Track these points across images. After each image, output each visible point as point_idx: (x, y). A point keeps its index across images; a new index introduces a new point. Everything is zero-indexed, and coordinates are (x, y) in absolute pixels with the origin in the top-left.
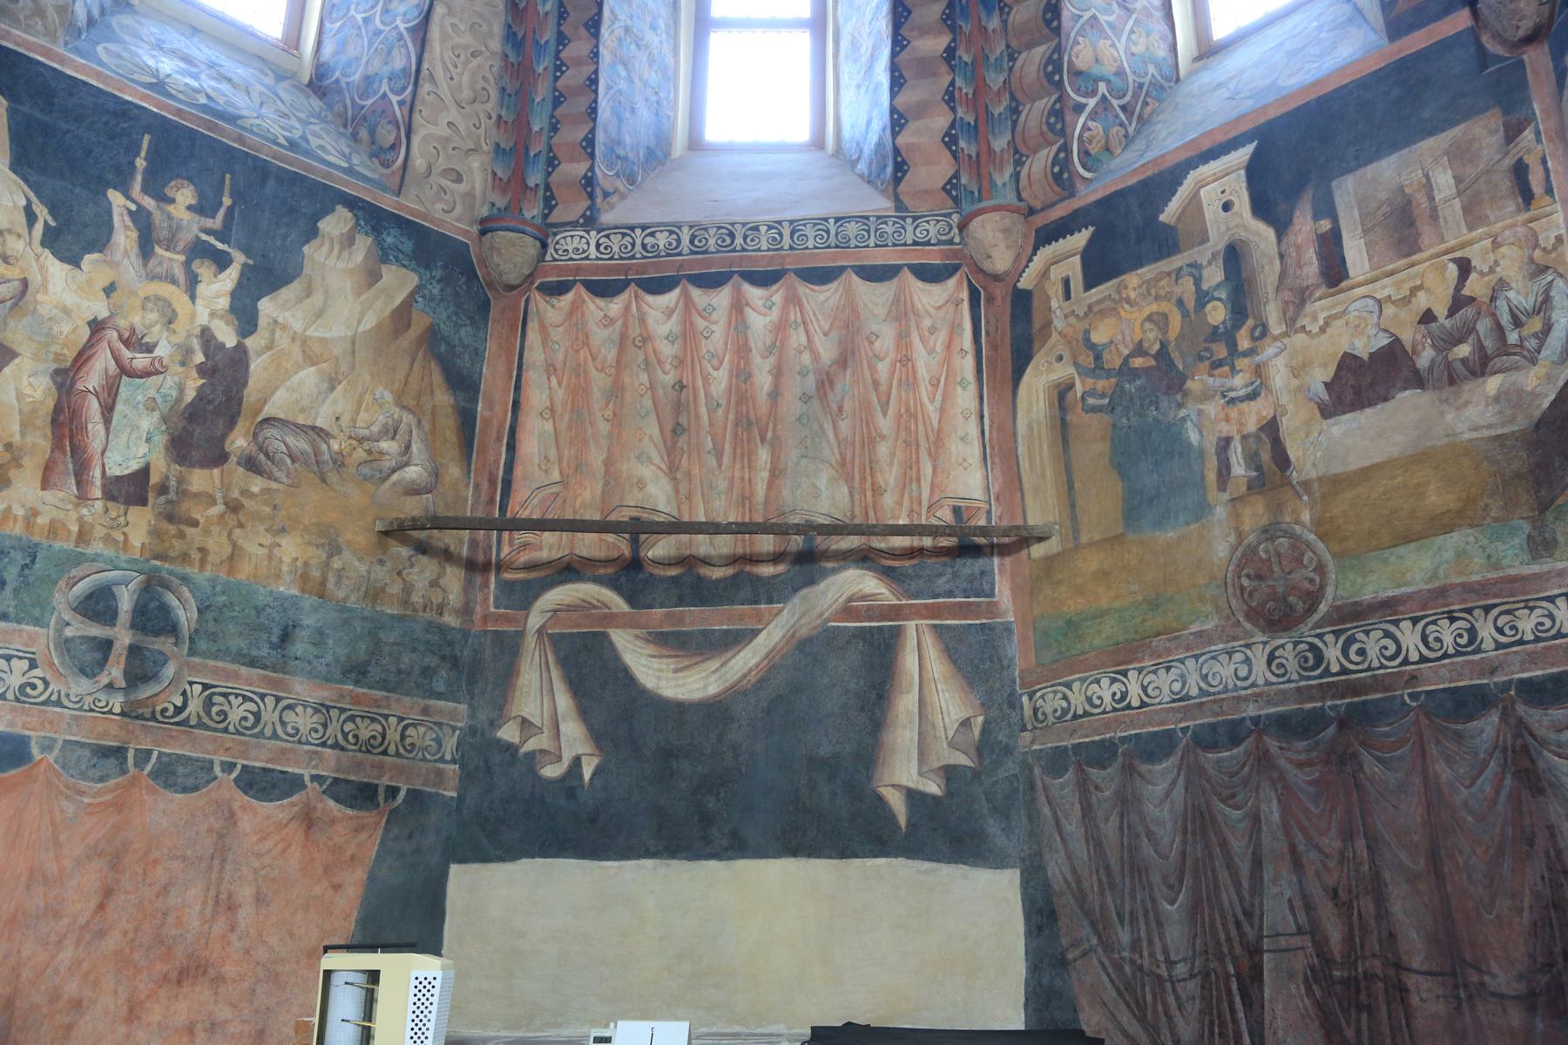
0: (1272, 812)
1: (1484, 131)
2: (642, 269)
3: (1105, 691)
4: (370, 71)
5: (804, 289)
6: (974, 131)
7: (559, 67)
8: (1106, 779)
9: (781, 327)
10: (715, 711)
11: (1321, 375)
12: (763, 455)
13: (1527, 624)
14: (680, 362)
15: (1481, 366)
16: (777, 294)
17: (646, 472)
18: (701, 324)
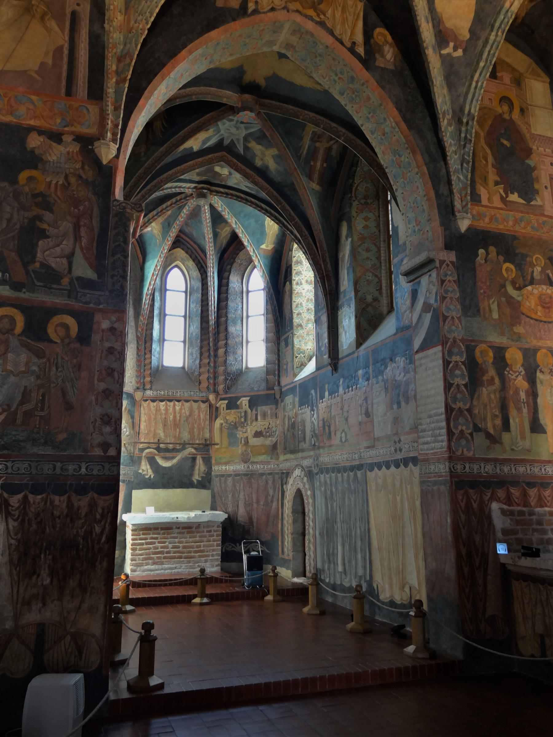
0: (242, 485)
1: (274, 407)
2: (159, 397)
3: (224, 468)
5: (185, 403)
8: (223, 479)
9: (181, 409)
10: (170, 468)
11: (253, 432)
12: (178, 430)
13: (269, 466)
14: (165, 414)
15: (269, 436)
16: (180, 403)
17: (160, 432)
18: (169, 408)
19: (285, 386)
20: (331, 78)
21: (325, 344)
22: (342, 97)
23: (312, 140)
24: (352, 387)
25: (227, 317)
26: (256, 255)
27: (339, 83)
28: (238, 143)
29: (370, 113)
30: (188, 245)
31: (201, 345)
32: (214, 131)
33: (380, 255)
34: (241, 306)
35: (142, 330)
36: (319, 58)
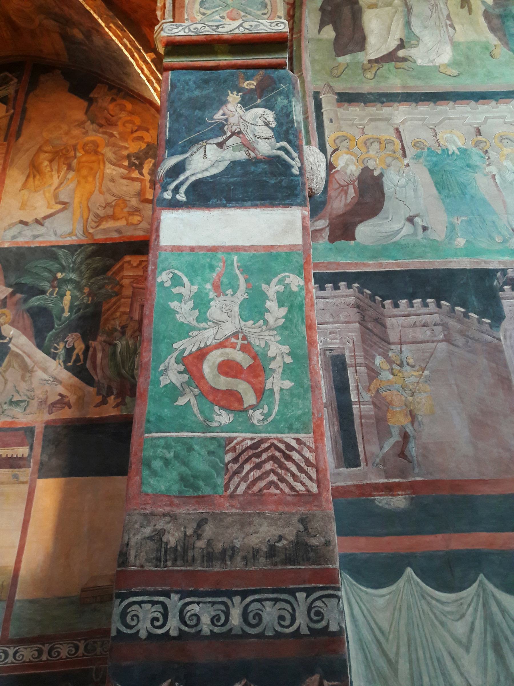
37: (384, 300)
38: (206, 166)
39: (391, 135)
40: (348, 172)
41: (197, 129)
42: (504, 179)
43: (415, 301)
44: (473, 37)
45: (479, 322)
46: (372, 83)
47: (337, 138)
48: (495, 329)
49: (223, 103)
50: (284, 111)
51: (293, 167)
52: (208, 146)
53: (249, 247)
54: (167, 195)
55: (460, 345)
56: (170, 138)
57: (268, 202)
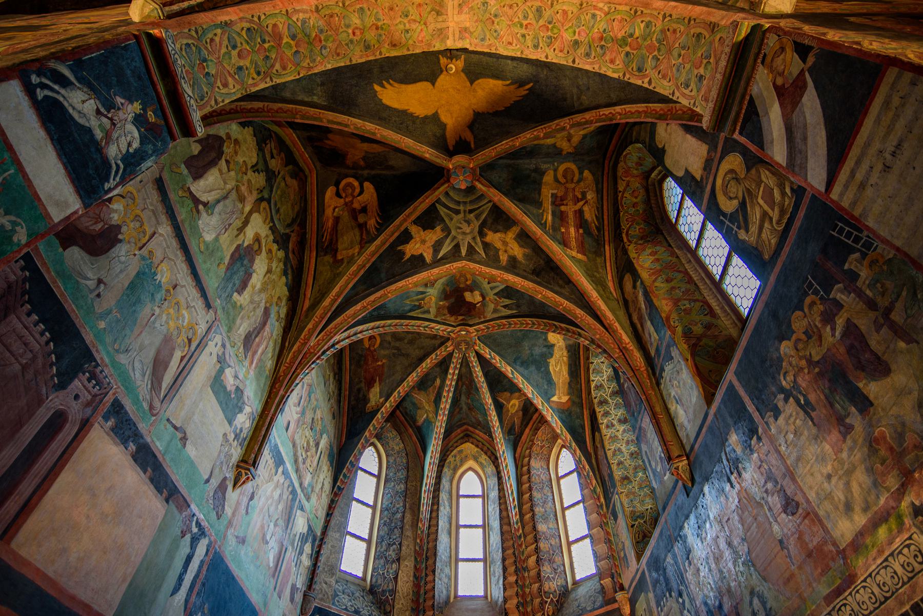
4: (385, 587)
6: (523, 605)
7: (426, 583)
19: (630, 587)
20: (518, 35)
21: (660, 458)
22: (539, 50)
23: (553, 203)
24: (729, 480)
25: (532, 510)
26: (547, 409)
27: (529, 35)
28: (476, 243)
29: (575, 32)
30: (477, 437)
31: (503, 556)
32: (442, 230)
33: (691, 278)
34: (551, 497)
35: (421, 540)
36: (496, 21)
37: (27, 302)
38: (76, 106)
39: (149, 232)
40: (111, 216)
41: (102, 85)
42: (154, 323)
43: (41, 325)
44: (224, 247)
45: (52, 377)
46: (177, 198)
47: (131, 193)
48: (53, 390)
49: (131, 101)
50: (144, 154)
51: (108, 182)
52: (92, 101)
53: (29, 179)
54: (34, 79)
55: (26, 378)
56: (84, 61)
57: (74, 176)
